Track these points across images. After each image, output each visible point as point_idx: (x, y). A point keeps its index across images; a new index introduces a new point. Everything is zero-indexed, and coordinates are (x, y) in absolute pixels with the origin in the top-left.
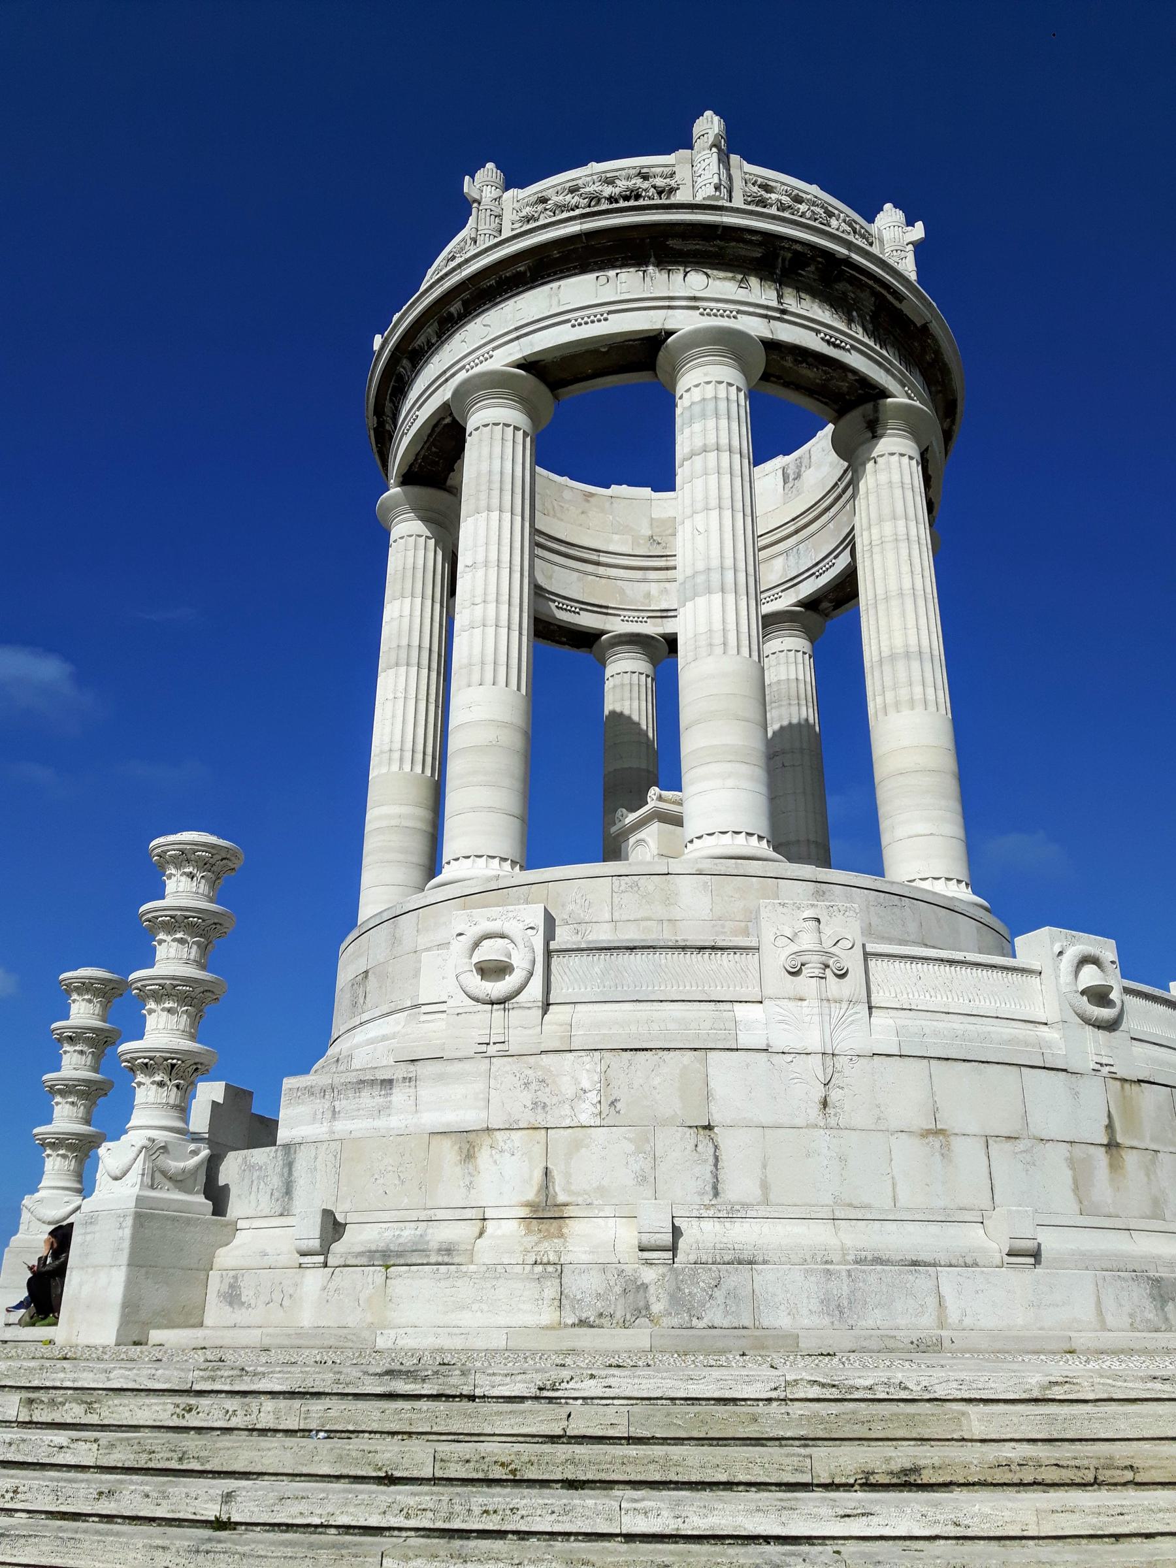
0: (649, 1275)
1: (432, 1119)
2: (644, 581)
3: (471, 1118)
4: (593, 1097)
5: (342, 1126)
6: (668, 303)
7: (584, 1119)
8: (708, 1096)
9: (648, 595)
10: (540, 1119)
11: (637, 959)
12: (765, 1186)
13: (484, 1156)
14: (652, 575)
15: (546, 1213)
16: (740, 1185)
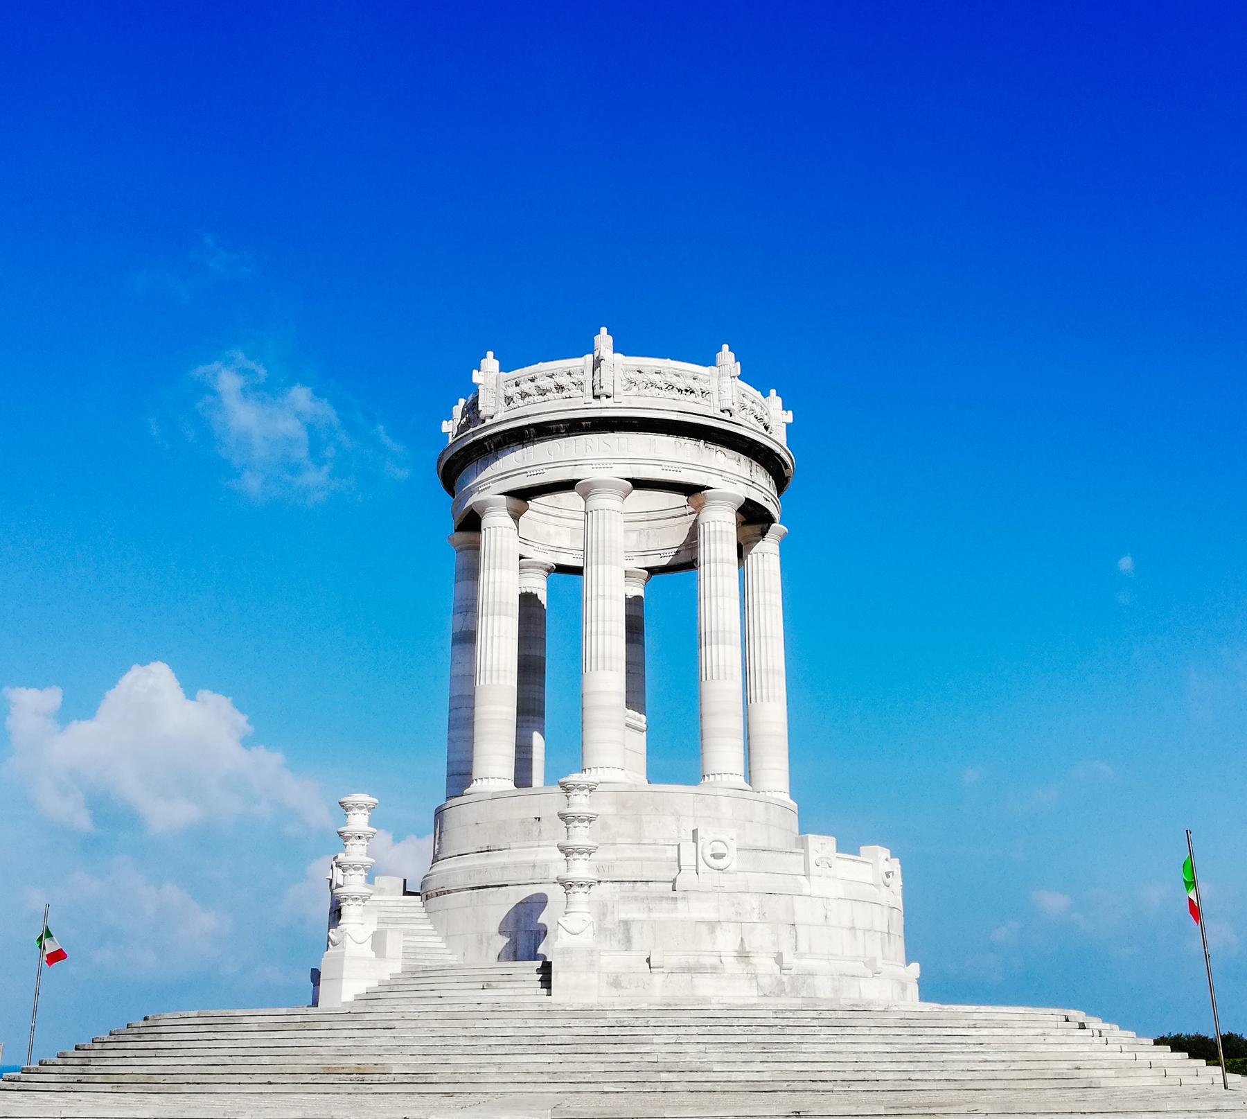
0: (785, 979)
1: (697, 915)
2: (548, 523)
3: (712, 916)
4: (757, 911)
5: (654, 915)
6: (709, 470)
7: (755, 918)
8: (794, 913)
9: (548, 534)
10: (738, 919)
11: (765, 854)
12: (810, 947)
13: (719, 932)
14: (552, 520)
15: (743, 955)
16: (803, 947)
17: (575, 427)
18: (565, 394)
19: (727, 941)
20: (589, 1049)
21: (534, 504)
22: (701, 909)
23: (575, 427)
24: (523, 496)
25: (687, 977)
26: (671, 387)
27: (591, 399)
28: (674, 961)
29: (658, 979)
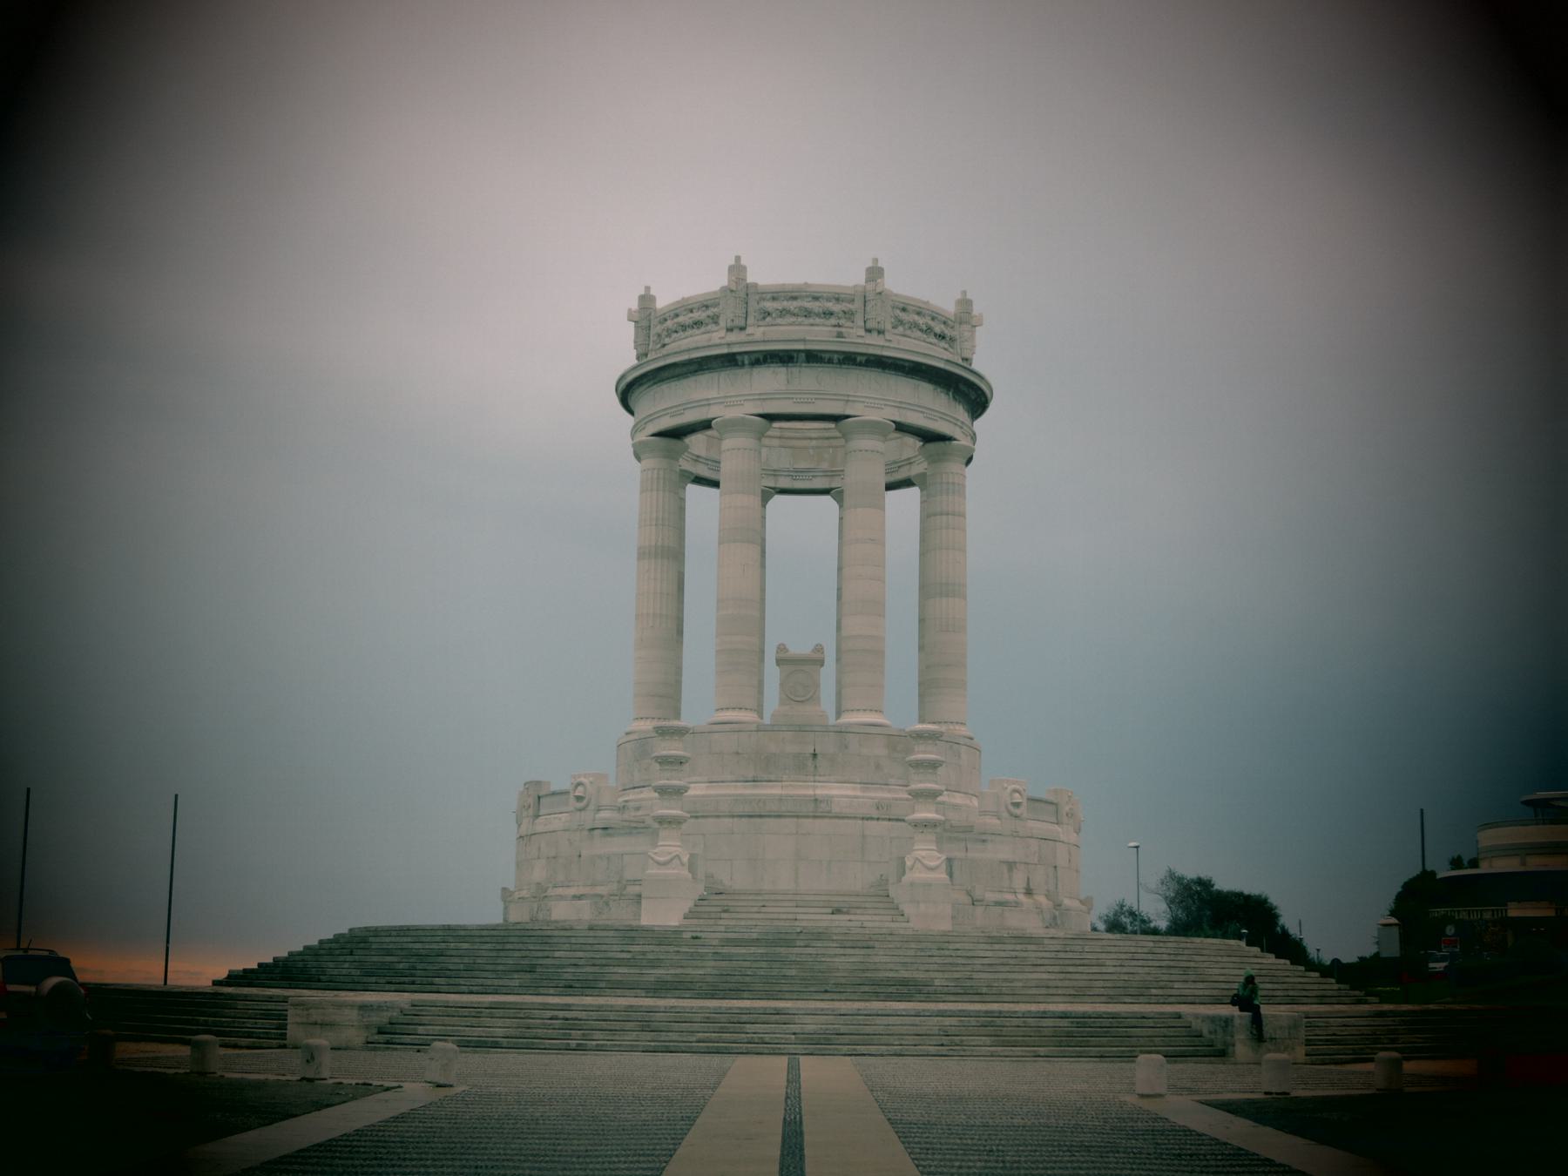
6: (954, 422)
15: (1029, 892)
17: (849, 360)
18: (833, 321)
19: (1019, 882)
20: (1071, 969)
21: (776, 425)
22: (1003, 851)
23: (849, 360)
24: (770, 418)
25: (998, 909)
26: (929, 330)
27: (862, 332)
28: (991, 897)
29: (979, 910)
